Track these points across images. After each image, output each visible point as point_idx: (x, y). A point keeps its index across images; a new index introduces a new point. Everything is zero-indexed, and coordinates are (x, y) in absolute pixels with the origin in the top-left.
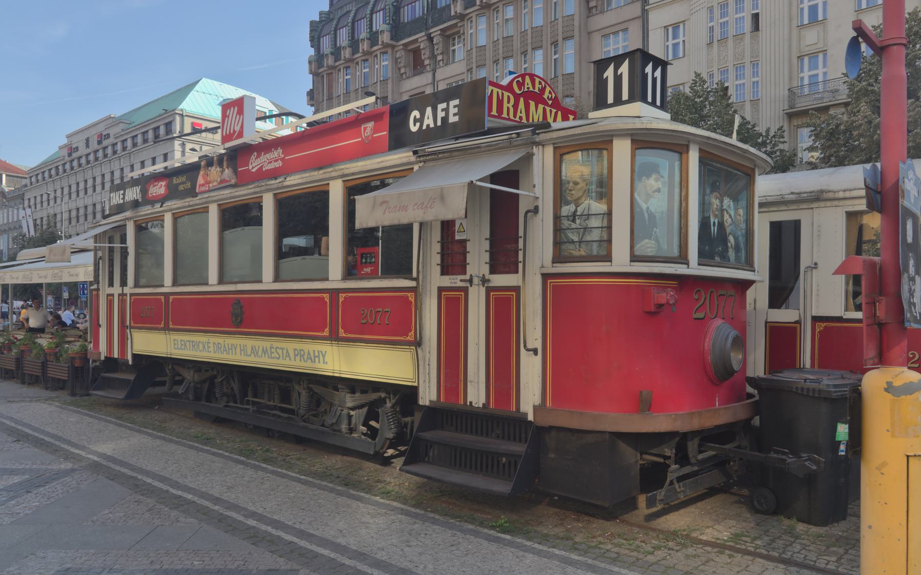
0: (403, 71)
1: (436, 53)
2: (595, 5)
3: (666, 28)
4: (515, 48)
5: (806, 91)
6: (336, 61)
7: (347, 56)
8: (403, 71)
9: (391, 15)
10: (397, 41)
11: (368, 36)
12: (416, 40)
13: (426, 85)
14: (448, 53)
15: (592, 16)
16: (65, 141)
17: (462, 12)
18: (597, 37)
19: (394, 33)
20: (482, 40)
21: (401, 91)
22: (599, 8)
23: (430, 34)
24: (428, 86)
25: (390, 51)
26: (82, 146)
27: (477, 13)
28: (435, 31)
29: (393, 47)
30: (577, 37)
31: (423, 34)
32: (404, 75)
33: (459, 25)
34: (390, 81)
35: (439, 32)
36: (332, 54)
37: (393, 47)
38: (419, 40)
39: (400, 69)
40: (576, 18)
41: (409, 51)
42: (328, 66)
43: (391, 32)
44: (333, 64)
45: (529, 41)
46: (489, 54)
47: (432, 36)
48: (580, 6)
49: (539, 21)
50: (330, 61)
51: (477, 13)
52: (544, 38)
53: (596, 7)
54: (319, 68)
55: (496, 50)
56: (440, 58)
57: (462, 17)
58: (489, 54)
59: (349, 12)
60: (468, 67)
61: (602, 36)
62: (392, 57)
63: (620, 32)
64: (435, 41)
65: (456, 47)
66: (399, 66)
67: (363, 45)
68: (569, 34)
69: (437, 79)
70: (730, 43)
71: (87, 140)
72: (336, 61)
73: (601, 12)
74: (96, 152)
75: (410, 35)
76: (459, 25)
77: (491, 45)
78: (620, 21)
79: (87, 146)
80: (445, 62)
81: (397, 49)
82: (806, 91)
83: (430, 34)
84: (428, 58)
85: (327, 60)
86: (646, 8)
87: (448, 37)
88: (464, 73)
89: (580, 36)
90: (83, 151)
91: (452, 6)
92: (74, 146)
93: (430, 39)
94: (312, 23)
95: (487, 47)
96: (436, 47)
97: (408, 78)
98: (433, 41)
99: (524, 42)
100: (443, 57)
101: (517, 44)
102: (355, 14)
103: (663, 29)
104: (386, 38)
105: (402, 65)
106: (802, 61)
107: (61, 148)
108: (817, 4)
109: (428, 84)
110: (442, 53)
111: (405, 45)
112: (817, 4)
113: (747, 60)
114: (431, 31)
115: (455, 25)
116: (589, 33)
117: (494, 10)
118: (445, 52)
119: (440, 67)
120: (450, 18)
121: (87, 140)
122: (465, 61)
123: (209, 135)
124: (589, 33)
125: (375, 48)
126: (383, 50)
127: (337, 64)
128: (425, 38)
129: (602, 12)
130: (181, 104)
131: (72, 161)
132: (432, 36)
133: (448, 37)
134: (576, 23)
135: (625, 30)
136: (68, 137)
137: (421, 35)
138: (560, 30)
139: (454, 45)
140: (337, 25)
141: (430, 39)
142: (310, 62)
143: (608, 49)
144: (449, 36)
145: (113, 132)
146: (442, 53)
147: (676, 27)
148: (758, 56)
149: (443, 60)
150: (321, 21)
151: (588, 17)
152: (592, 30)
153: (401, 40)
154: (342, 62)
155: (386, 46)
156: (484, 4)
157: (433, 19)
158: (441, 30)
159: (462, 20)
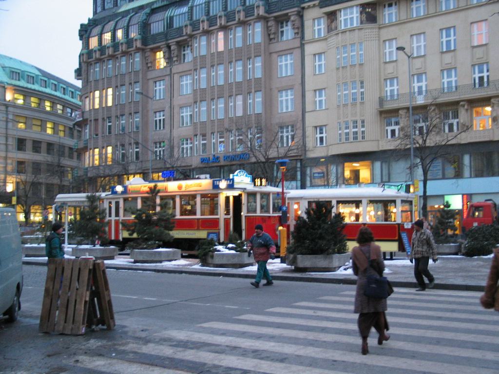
3: (315, 55)
5: (389, 99)
6: (101, 55)
7: (110, 53)
10: (146, 46)
20: (203, 52)
21: (148, 77)
23: (169, 43)
29: (143, 50)
31: (164, 43)
33: (188, 40)
34: (141, 72)
38: (161, 47)
39: (147, 64)
48: (264, 38)
56: (175, 59)
64: (172, 48)
65: (186, 52)
69: (173, 72)
70: (348, 68)
73: (276, 42)
82: (389, 99)
85: (96, 54)
88: (191, 70)
94: (82, 25)
95: (207, 56)
96: (172, 52)
103: (313, 56)
106: (386, 81)
109: (167, 75)
110: (177, 56)
113: (357, 79)
114: (170, 41)
115: (186, 40)
116: (271, 53)
122: (193, 62)
124: (271, 53)
127: (103, 57)
128: (166, 46)
129: (278, 42)
134: (262, 48)
139: (184, 51)
143: (281, 63)
146: (177, 56)
147: (320, 54)
148: (363, 77)
151: (269, 44)
152: (272, 51)
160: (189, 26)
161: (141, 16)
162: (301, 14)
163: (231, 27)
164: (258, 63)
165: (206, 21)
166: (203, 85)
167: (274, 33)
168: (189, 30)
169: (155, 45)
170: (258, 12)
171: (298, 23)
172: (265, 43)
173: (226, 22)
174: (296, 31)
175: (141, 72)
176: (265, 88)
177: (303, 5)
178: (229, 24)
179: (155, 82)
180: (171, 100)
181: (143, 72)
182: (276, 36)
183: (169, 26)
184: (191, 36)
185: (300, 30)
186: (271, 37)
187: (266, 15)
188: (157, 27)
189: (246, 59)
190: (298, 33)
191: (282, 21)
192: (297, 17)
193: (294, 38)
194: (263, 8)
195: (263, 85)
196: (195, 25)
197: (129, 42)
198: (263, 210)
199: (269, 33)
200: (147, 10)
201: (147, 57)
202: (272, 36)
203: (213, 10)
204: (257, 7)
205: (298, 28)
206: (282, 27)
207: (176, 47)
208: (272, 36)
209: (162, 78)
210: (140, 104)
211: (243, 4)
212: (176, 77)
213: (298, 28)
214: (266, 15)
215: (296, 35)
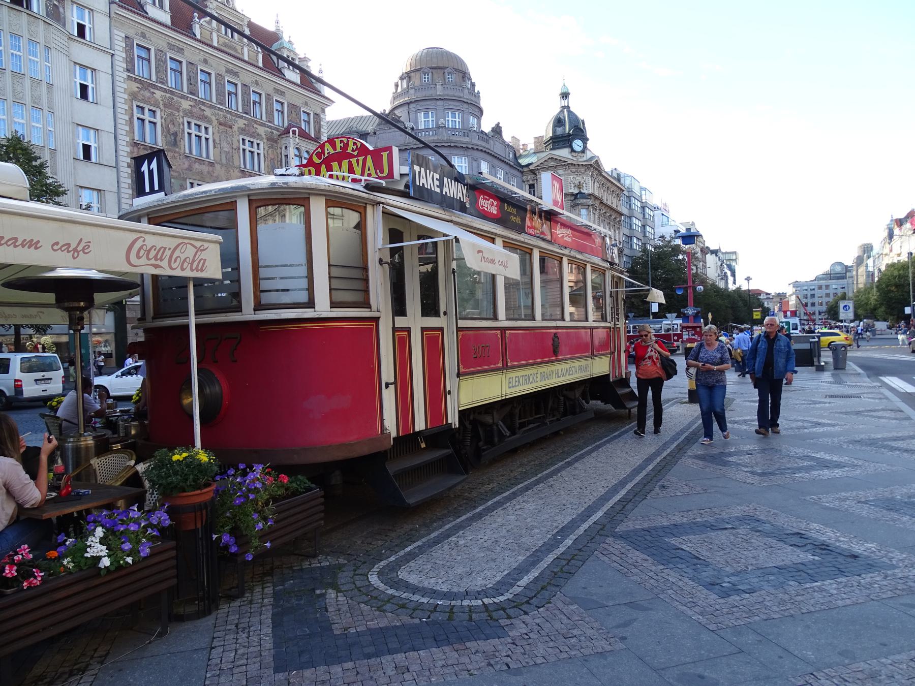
108: (83, 144)
112: (83, 144)
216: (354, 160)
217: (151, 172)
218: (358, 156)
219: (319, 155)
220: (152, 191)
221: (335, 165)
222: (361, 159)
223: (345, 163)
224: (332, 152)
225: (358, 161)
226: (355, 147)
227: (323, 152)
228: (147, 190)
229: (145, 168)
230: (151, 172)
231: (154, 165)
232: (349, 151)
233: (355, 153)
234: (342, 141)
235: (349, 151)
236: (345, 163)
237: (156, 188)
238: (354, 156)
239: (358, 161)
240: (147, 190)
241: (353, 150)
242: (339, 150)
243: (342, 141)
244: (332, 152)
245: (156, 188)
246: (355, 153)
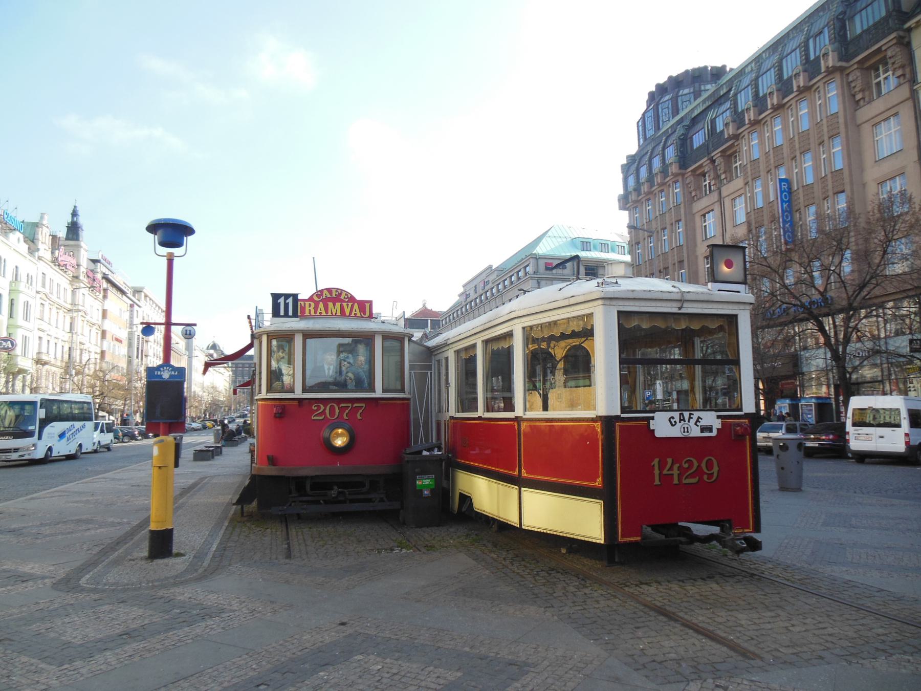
0: (693, 194)
1: (719, 174)
2: (861, 97)
4: (785, 155)
8: (693, 194)
9: (679, 148)
11: (661, 170)
12: (701, 166)
13: (714, 203)
14: (731, 171)
15: (860, 108)
16: (462, 290)
17: (735, 133)
18: (866, 128)
19: (682, 163)
20: (756, 154)
22: (867, 99)
23: (712, 157)
24: (716, 204)
25: (680, 178)
26: (472, 292)
27: (748, 130)
28: (716, 154)
30: (843, 134)
31: (706, 159)
32: (695, 198)
34: (682, 206)
35: (719, 154)
36: (635, 190)
37: (683, 175)
40: (841, 115)
41: (699, 175)
42: (632, 201)
43: (679, 162)
44: (636, 199)
45: (797, 146)
46: (762, 167)
47: (714, 158)
48: (844, 102)
49: (805, 125)
50: (633, 197)
51: (748, 130)
52: (812, 140)
53: (863, 98)
54: (626, 204)
55: (768, 161)
56: (723, 176)
57: (736, 137)
58: (762, 167)
59: (647, 152)
60: (746, 181)
61: (873, 126)
62: (683, 184)
63: (892, 118)
66: (690, 190)
67: (657, 178)
68: (835, 132)
71: (476, 287)
72: (638, 196)
73: (869, 102)
74: (481, 296)
75: (696, 162)
76: (736, 144)
77: (764, 157)
78: (889, 107)
79: (476, 292)
80: (728, 180)
81: (686, 176)
83: (712, 157)
84: (723, 173)
86: (915, 88)
87: (730, 156)
88: (742, 188)
89: (847, 132)
90: (473, 296)
91: (725, 130)
92: (467, 293)
93: (713, 161)
97: (698, 199)
98: (715, 162)
99: (792, 149)
100: (726, 175)
101: (786, 151)
102: (652, 153)
104: (674, 169)
105: (692, 189)
107: (460, 296)
110: (725, 172)
111: (694, 171)
114: (713, 155)
115: (732, 146)
116: (859, 126)
117: (764, 124)
118: (728, 170)
119: (724, 185)
120: (727, 141)
121: (476, 287)
123: (559, 271)
124: (859, 126)
125: (668, 179)
126: (673, 180)
127: (640, 197)
128: (709, 161)
130: (535, 249)
131: (466, 305)
132: (714, 158)
133: (730, 156)
134: (841, 120)
135: (896, 114)
136: (464, 286)
137: (704, 161)
138: (825, 129)
139: (736, 162)
140: (638, 165)
141: (713, 161)
142: (619, 200)
144: (730, 156)
145: (491, 278)
146: (725, 172)
149: (726, 178)
150: (627, 164)
151: (856, 110)
153: (688, 168)
154: (643, 196)
155: (676, 175)
156: (752, 122)
157: (713, 144)
158: (721, 152)
159: (738, 140)
160: (731, 124)
161: (680, 131)
162: (906, 40)
163: (789, 104)
164: (837, 148)
165: (752, 108)
166: (760, 203)
167: (862, 90)
168: (731, 130)
169: (697, 165)
170: (827, 64)
171: (900, 59)
172: (845, 110)
173: (781, 97)
174: (899, 72)
175: (682, 206)
176: (852, 183)
177: (906, 26)
178: (786, 100)
179: (704, 215)
180: (723, 235)
181: (685, 206)
182: (867, 93)
183: (710, 133)
184: (736, 137)
185: (908, 70)
186: (854, 102)
187: (844, 64)
188: (698, 139)
189: (817, 146)
190: (904, 75)
191: (873, 65)
192: (898, 50)
193: (900, 85)
194: (836, 53)
195: (847, 180)
196: (738, 117)
197: (664, 171)
198: (277, 384)
199: (853, 92)
200: (687, 123)
201: (688, 184)
202: (859, 97)
203: (763, 85)
204: (823, 56)
205: (903, 67)
206: (878, 76)
207: (722, 160)
208: (859, 97)
209: (710, 208)
210: (685, 248)
211: (804, 61)
212: (727, 202)
213: (903, 67)
214: (844, 64)
215: (902, 78)
216: (345, 304)
217: (286, 305)
218: (347, 302)
219: (318, 296)
220: (286, 315)
221: (330, 304)
222: (350, 304)
223: (338, 305)
224: (329, 296)
225: (348, 305)
226: (346, 297)
227: (322, 295)
228: (282, 313)
229: (281, 301)
230: (286, 305)
231: (290, 301)
232: (342, 297)
233: (347, 300)
234: (336, 291)
235: (342, 297)
236: (338, 305)
237: (290, 313)
238: (345, 302)
239: (348, 305)
240: (282, 313)
241: (344, 298)
242: (334, 296)
243: (336, 291)
244: (329, 296)
245: (290, 313)
246: (347, 300)
